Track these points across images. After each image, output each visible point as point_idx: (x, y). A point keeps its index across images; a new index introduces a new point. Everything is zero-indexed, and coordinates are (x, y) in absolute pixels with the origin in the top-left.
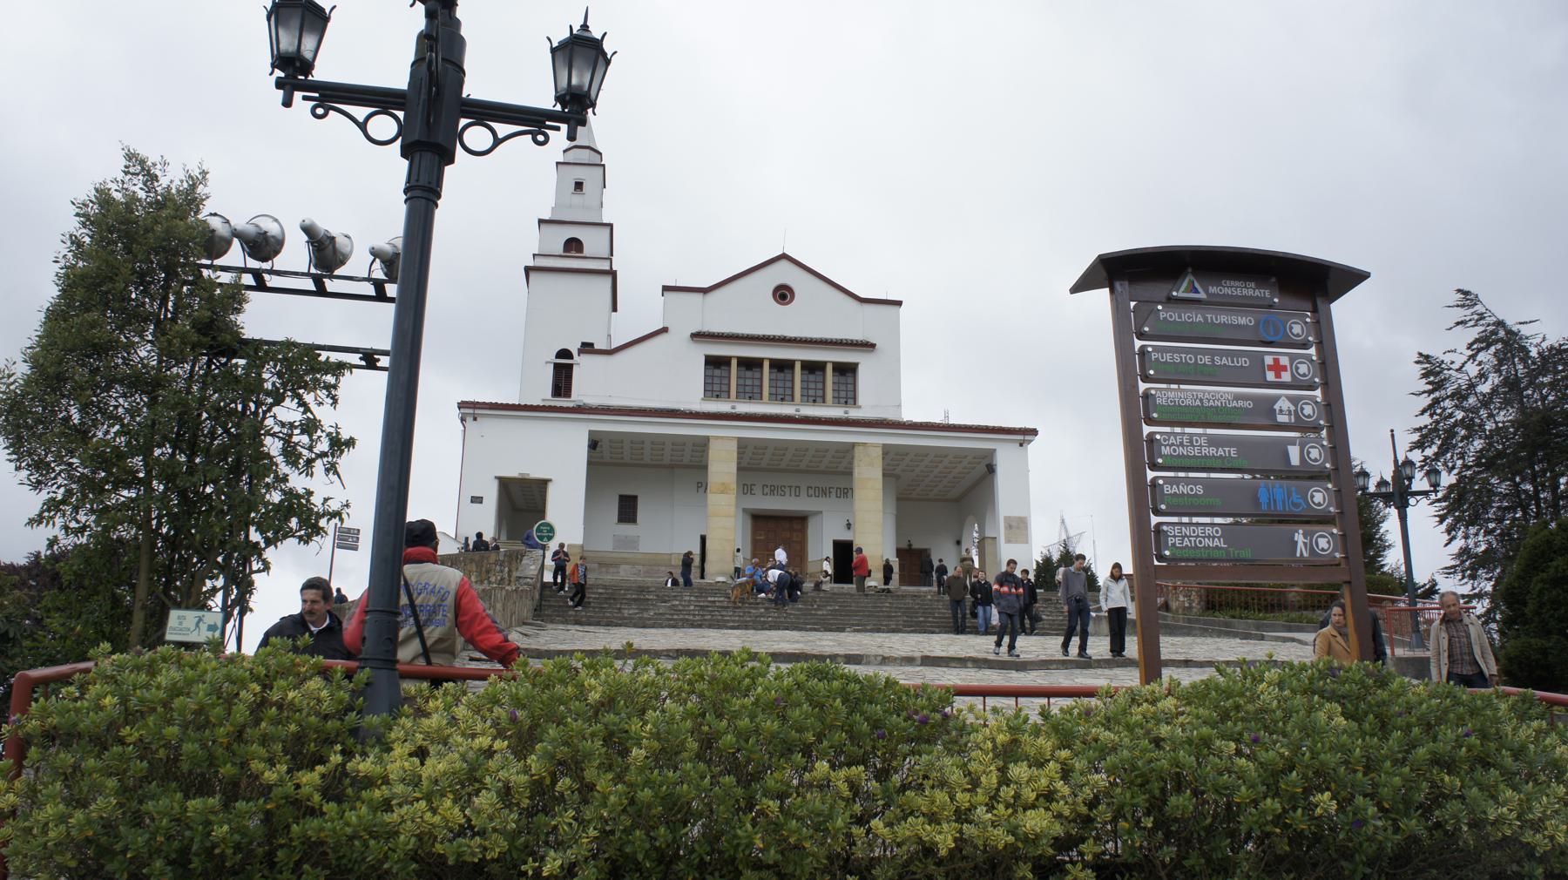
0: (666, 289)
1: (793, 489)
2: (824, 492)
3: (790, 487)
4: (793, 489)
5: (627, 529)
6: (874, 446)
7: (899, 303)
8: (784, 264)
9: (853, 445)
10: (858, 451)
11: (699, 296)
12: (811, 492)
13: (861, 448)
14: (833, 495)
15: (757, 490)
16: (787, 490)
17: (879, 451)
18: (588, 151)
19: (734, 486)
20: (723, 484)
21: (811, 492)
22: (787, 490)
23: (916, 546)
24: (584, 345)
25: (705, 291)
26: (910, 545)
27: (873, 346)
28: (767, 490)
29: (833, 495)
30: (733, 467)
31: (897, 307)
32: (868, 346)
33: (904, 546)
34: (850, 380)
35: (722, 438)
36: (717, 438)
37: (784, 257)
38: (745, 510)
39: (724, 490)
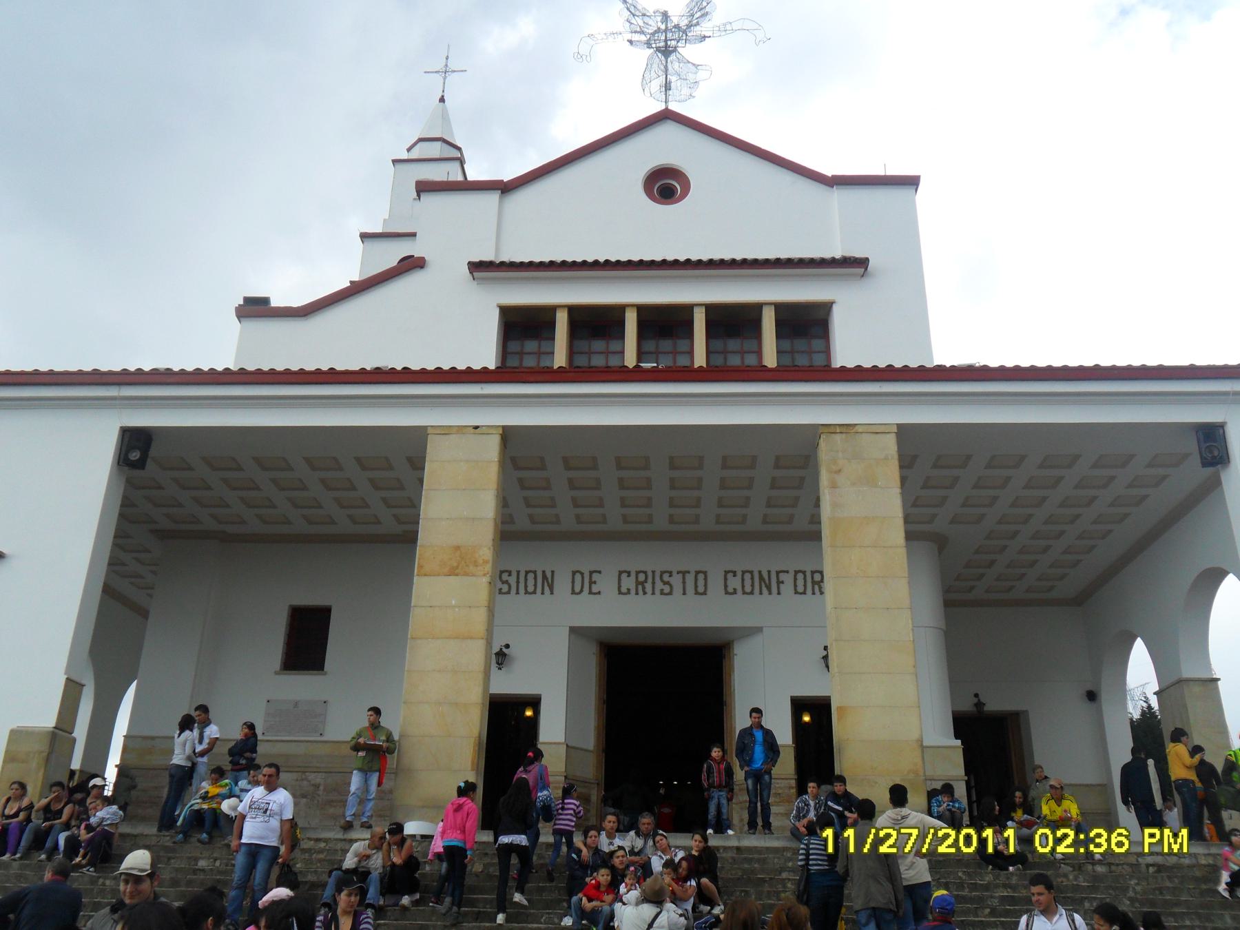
1: (690, 579)
2: (766, 583)
3: (684, 573)
4: (690, 579)
5: (302, 686)
6: (876, 430)
7: (912, 182)
8: (668, 129)
9: (812, 434)
11: (494, 197)
12: (734, 583)
14: (787, 588)
15: (606, 583)
16: (676, 581)
17: (890, 444)
18: (439, 144)
19: (486, 553)
20: (458, 548)
21: (734, 583)
22: (676, 581)
23: (993, 705)
24: (249, 301)
26: (979, 705)
27: (862, 263)
28: (628, 583)
29: (787, 588)
30: (486, 505)
31: (911, 190)
32: (855, 265)
33: (967, 706)
34: (817, 344)
36: (446, 431)
37: (666, 116)
38: (574, 631)
39: (459, 564)
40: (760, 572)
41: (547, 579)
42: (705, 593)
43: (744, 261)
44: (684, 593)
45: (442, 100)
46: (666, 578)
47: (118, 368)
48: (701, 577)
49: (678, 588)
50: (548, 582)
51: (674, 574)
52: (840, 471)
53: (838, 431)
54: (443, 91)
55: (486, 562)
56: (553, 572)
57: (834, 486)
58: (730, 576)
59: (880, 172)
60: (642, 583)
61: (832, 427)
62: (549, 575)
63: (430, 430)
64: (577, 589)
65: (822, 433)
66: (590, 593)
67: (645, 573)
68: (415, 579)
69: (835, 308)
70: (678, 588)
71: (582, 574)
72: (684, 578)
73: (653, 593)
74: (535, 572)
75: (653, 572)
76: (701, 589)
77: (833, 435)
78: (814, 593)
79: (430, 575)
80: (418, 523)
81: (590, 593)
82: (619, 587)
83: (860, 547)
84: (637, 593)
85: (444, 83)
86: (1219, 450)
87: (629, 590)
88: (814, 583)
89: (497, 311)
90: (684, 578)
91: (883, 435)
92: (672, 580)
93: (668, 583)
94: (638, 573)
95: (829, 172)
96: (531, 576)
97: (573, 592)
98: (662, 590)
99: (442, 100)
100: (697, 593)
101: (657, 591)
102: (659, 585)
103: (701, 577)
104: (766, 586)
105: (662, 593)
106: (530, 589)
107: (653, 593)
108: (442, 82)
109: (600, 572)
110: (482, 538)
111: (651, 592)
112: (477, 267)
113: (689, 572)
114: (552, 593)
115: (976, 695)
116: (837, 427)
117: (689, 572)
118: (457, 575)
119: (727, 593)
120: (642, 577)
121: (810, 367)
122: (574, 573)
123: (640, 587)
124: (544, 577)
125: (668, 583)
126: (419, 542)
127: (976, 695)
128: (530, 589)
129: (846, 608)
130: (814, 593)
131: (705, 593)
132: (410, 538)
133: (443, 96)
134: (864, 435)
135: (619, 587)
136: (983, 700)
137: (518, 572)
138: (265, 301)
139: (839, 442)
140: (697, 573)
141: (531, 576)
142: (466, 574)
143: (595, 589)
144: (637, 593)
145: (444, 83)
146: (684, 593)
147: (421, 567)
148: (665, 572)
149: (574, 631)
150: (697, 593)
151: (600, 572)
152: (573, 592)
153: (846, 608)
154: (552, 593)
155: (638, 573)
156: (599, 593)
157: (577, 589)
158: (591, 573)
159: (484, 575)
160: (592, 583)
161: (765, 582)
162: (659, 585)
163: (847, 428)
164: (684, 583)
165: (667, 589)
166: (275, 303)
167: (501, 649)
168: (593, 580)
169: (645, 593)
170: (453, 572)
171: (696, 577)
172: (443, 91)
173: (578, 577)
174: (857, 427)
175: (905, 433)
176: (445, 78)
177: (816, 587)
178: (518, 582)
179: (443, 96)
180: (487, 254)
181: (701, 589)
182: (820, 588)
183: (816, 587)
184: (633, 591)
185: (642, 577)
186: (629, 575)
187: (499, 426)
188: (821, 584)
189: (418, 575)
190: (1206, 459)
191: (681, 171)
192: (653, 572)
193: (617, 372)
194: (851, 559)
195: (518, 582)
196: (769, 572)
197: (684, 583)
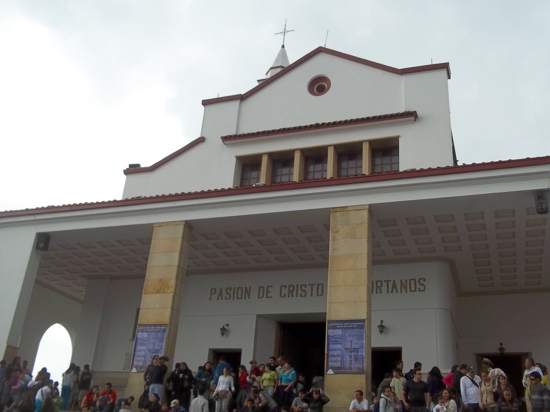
0: (206, 103)
1: (315, 288)
3: (312, 285)
4: (315, 288)
6: (358, 209)
8: (322, 57)
9: (327, 213)
10: (335, 221)
13: (338, 214)
16: (308, 289)
20: (161, 280)
22: (308, 289)
25: (242, 98)
26: (501, 349)
28: (285, 291)
35: (167, 224)
36: (161, 225)
37: (320, 50)
40: (246, 288)
41: (247, 291)
42: (322, 295)
43: (323, 124)
44: (312, 296)
45: (283, 47)
46: (303, 288)
47: (24, 209)
48: (320, 287)
49: (309, 294)
50: (248, 292)
51: (307, 285)
52: (338, 231)
53: (339, 211)
54: (284, 42)
55: (172, 286)
56: (250, 287)
57: (334, 239)
58: (283, 288)
59: (429, 63)
60: (292, 292)
61: (336, 208)
62: (248, 289)
63: (155, 225)
64: (261, 296)
65: (331, 212)
66: (267, 297)
67: (293, 286)
68: (143, 295)
69: (400, 139)
70: (309, 294)
71: (264, 288)
72: (312, 287)
73: (297, 296)
74: (242, 288)
75: (297, 286)
76: (320, 293)
77: (336, 213)
78: (377, 293)
79: (149, 294)
80: (146, 269)
81: (267, 297)
82: (281, 294)
83: (344, 270)
84: (289, 297)
85: (284, 38)
86: (545, 203)
87: (285, 295)
88: (377, 287)
89: (235, 159)
90: (312, 287)
91: (362, 211)
92: (306, 289)
93: (303, 291)
94: (290, 286)
95: (400, 67)
96: (240, 290)
97: (259, 297)
98: (301, 294)
99: (283, 47)
100: (318, 295)
101: (299, 295)
102: (300, 292)
103: (320, 287)
104: (248, 294)
105: (301, 295)
106: (240, 296)
107: (297, 296)
108: (283, 37)
109: (272, 287)
110: (171, 275)
111: (295, 296)
112: (225, 139)
113: (315, 285)
114: (249, 298)
115: (501, 344)
116: (339, 209)
117: (315, 285)
118: (159, 293)
119: (281, 296)
120: (291, 288)
121: (355, 176)
122: (260, 288)
123: (290, 293)
124: (246, 291)
125: (423, 285)
126: (146, 278)
127: (501, 344)
128: (240, 296)
129: (334, 303)
130: (377, 293)
131: (322, 295)
132: (143, 277)
133: (283, 45)
134: (352, 211)
135: (281, 294)
136: (503, 346)
137: (234, 288)
138: (138, 165)
139: (339, 216)
140: (319, 285)
141: (240, 290)
142: (163, 292)
143: (269, 295)
144: (289, 297)
145: (284, 38)
146: (312, 296)
147: (145, 290)
148: (303, 285)
149: (259, 316)
150: (318, 295)
151: (272, 287)
152: (259, 297)
153: (334, 303)
154: (249, 298)
155: (290, 286)
156: (271, 297)
157: (261, 296)
158: (268, 287)
159: (171, 293)
160: (268, 292)
161: (248, 293)
162: (300, 292)
163: (343, 209)
164: (312, 290)
165: (303, 294)
166: (142, 166)
167: (224, 327)
168: (269, 290)
169: (293, 296)
170: (158, 292)
171: (318, 286)
172: (284, 42)
173: (262, 289)
174: (349, 208)
175: (372, 209)
176: (284, 35)
177: (378, 290)
178: (234, 293)
179: (283, 45)
180: (232, 132)
181: (320, 293)
182: (380, 290)
183: (378, 290)
184: (287, 295)
185: (291, 288)
186: (285, 287)
187: (184, 221)
188: (381, 287)
189: (144, 294)
190: (538, 210)
191: (325, 77)
192: (297, 286)
193: (136, 200)
194: (339, 277)
195: (234, 293)
196: (406, 280)
197: (312, 290)
